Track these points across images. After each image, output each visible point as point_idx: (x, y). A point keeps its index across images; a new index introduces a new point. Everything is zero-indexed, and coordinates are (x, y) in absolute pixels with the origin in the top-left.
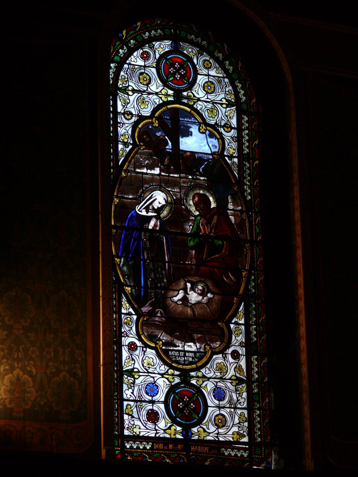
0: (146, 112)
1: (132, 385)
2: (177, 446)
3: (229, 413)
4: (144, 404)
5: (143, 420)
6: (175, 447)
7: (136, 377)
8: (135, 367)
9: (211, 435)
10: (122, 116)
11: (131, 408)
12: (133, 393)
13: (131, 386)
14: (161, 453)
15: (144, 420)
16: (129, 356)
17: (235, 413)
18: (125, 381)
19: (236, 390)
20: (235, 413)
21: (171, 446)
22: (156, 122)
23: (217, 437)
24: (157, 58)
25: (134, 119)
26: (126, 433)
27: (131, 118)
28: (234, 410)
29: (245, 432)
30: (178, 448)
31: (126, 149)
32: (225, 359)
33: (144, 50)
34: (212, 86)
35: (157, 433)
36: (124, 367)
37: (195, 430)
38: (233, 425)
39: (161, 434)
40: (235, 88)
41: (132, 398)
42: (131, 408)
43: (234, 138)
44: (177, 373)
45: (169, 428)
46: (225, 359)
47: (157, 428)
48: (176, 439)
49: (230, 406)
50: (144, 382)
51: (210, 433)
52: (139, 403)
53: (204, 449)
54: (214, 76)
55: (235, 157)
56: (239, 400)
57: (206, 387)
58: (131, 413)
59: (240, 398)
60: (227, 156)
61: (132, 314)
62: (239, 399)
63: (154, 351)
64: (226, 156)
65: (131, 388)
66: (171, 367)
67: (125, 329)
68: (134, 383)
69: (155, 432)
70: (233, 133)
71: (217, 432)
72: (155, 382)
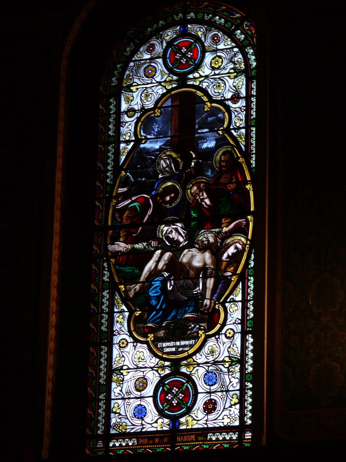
0: (150, 104)
1: (121, 383)
2: (164, 439)
3: (220, 397)
4: (131, 400)
5: (130, 417)
6: (161, 440)
7: (124, 374)
8: (124, 364)
9: (199, 422)
10: (125, 115)
11: (118, 406)
12: (121, 391)
13: (120, 384)
14: (147, 448)
15: (131, 416)
16: (120, 354)
17: (227, 396)
18: (114, 380)
19: (229, 371)
20: (227, 396)
21: (157, 440)
22: (158, 112)
23: (206, 424)
24: (164, 48)
25: (138, 115)
26: (113, 432)
27: (134, 114)
28: (226, 393)
29: (237, 415)
30: (164, 441)
31: (128, 147)
32: (217, 341)
33: (151, 43)
34: (220, 60)
35: (143, 428)
36: (113, 367)
37: (183, 420)
38: (224, 408)
39: (148, 428)
40: (245, 55)
41: (120, 397)
42: (118, 406)
43: (242, 108)
44: (167, 363)
45: (156, 422)
46: (217, 341)
47: (144, 423)
48: (163, 432)
49: (222, 389)
50: (133, 377)
51: (198, 421)
52: (127, 400)
53: (190, 437)
54: (222, 50)
55: (243, 128)
56: (232, 382)
57: (196, 373)
58: (118, 411)
59: (232, 379)
60: (234, 129)
61: (124, 311)
62: (231, 381)
63: (145, 346)
64: (232, 129)
65: (120, 386)
66: (161, 358)
67: (117, 327)
68: (123, 380)
69: (142, 427)
70: (242, 103)
71: (206, 418)
72: (144, 376)
